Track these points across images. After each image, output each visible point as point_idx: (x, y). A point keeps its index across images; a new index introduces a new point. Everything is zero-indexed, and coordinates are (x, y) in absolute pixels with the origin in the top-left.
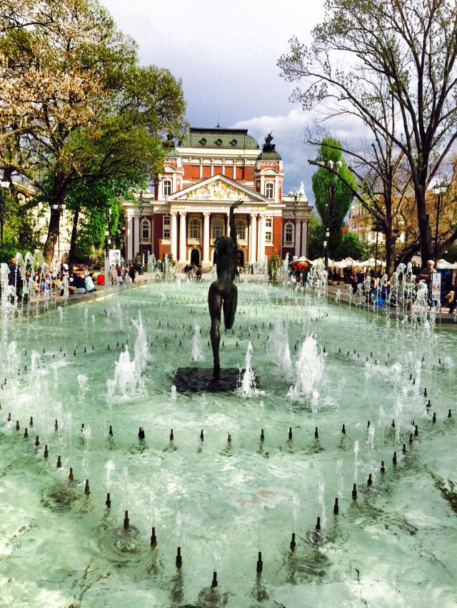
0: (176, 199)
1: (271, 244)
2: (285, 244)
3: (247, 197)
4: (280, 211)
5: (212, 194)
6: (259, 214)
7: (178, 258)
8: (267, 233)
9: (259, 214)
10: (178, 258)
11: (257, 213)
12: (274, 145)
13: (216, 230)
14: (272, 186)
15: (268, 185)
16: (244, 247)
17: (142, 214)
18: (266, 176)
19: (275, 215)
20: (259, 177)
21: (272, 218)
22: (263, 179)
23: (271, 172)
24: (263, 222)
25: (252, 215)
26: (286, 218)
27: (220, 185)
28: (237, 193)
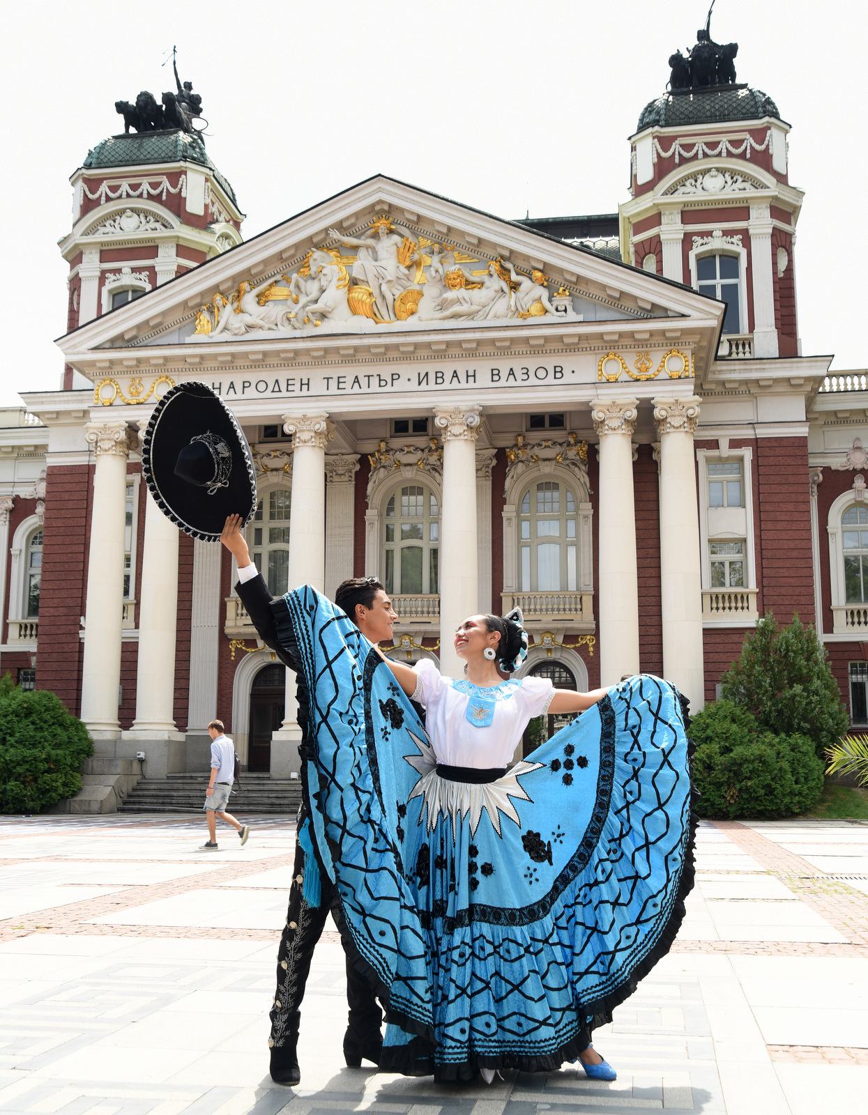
0: (119, 342)
1: (748, 618)
2: (839, 619)
3: (563, 301)
4: (794, 409)
5: (334, 296)
6: (646, 408)
7: (127, 713)
8: (716, 544)
9: (646, 408)
10: (127, 713)
11: (630, 396)
12: (732, 50)
13: (398, 545)
14: (730, 262)
15: (706, 264)
16: (570, 638)
17: (25, 492)
18: (689, 215)
19: (763, 432)
20: (655, 220)
21: (747, 453)
22: (671, 231)
23: (714, 189)
24: (676, 453)
25: (596, 415)
26: (837, 463)
27: (388, 246)
28: (497, 283)
